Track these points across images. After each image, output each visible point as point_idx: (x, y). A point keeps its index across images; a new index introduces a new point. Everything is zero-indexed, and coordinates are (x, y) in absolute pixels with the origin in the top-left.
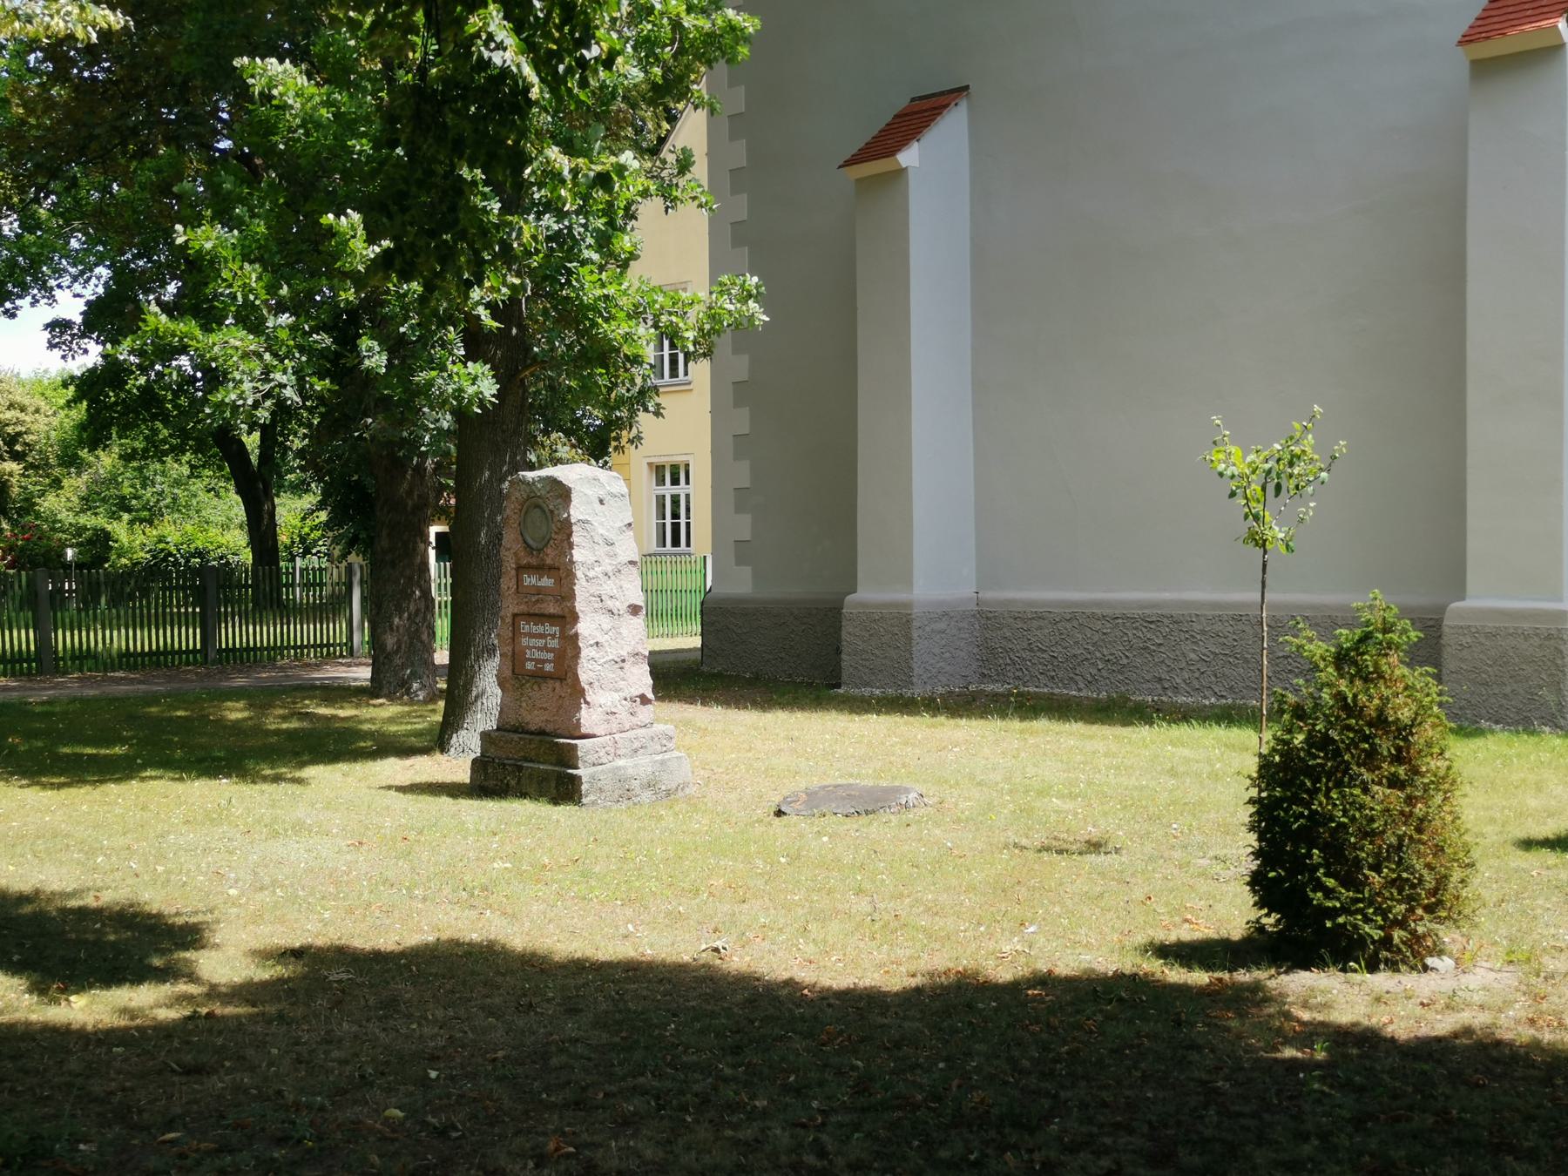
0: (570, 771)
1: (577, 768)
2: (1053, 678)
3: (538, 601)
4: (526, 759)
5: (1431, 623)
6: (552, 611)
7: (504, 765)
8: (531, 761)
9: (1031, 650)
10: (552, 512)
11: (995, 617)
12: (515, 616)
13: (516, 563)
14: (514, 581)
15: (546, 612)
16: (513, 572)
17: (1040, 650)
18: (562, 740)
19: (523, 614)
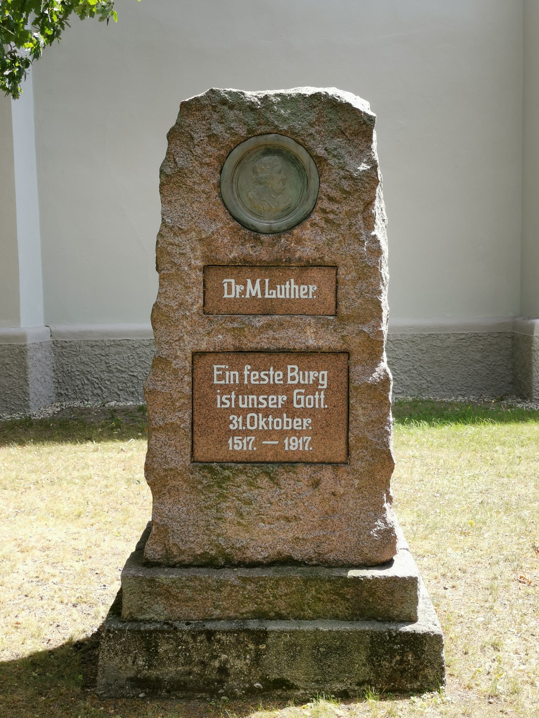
0: (408, 628)
1: (412, 620)
2: (133, 393)
3: (269, 326)
4: (262, 616)
5: (463, 337)
6: (312, 342)
7: (210, 634)
8: (280, 617)
9: (110, 372)
10: (319, 160)
11: (71, 346)
12: (197, 355)
13: (205, 257)
14: (197, 291)
15: (298, 346)
16: (197, 276)
17: (119, 371)
18: (352, 573)
19: (225, 352)
